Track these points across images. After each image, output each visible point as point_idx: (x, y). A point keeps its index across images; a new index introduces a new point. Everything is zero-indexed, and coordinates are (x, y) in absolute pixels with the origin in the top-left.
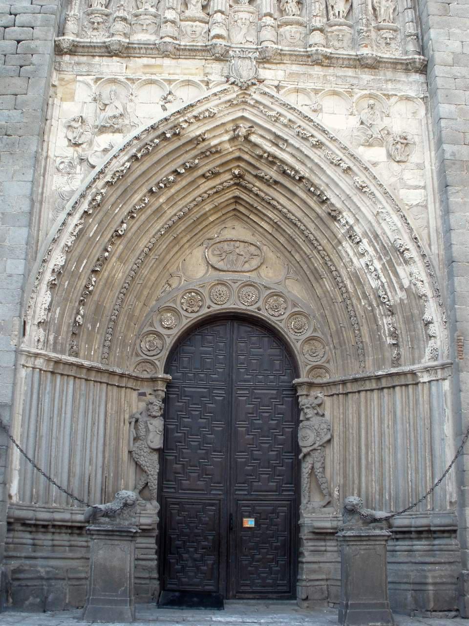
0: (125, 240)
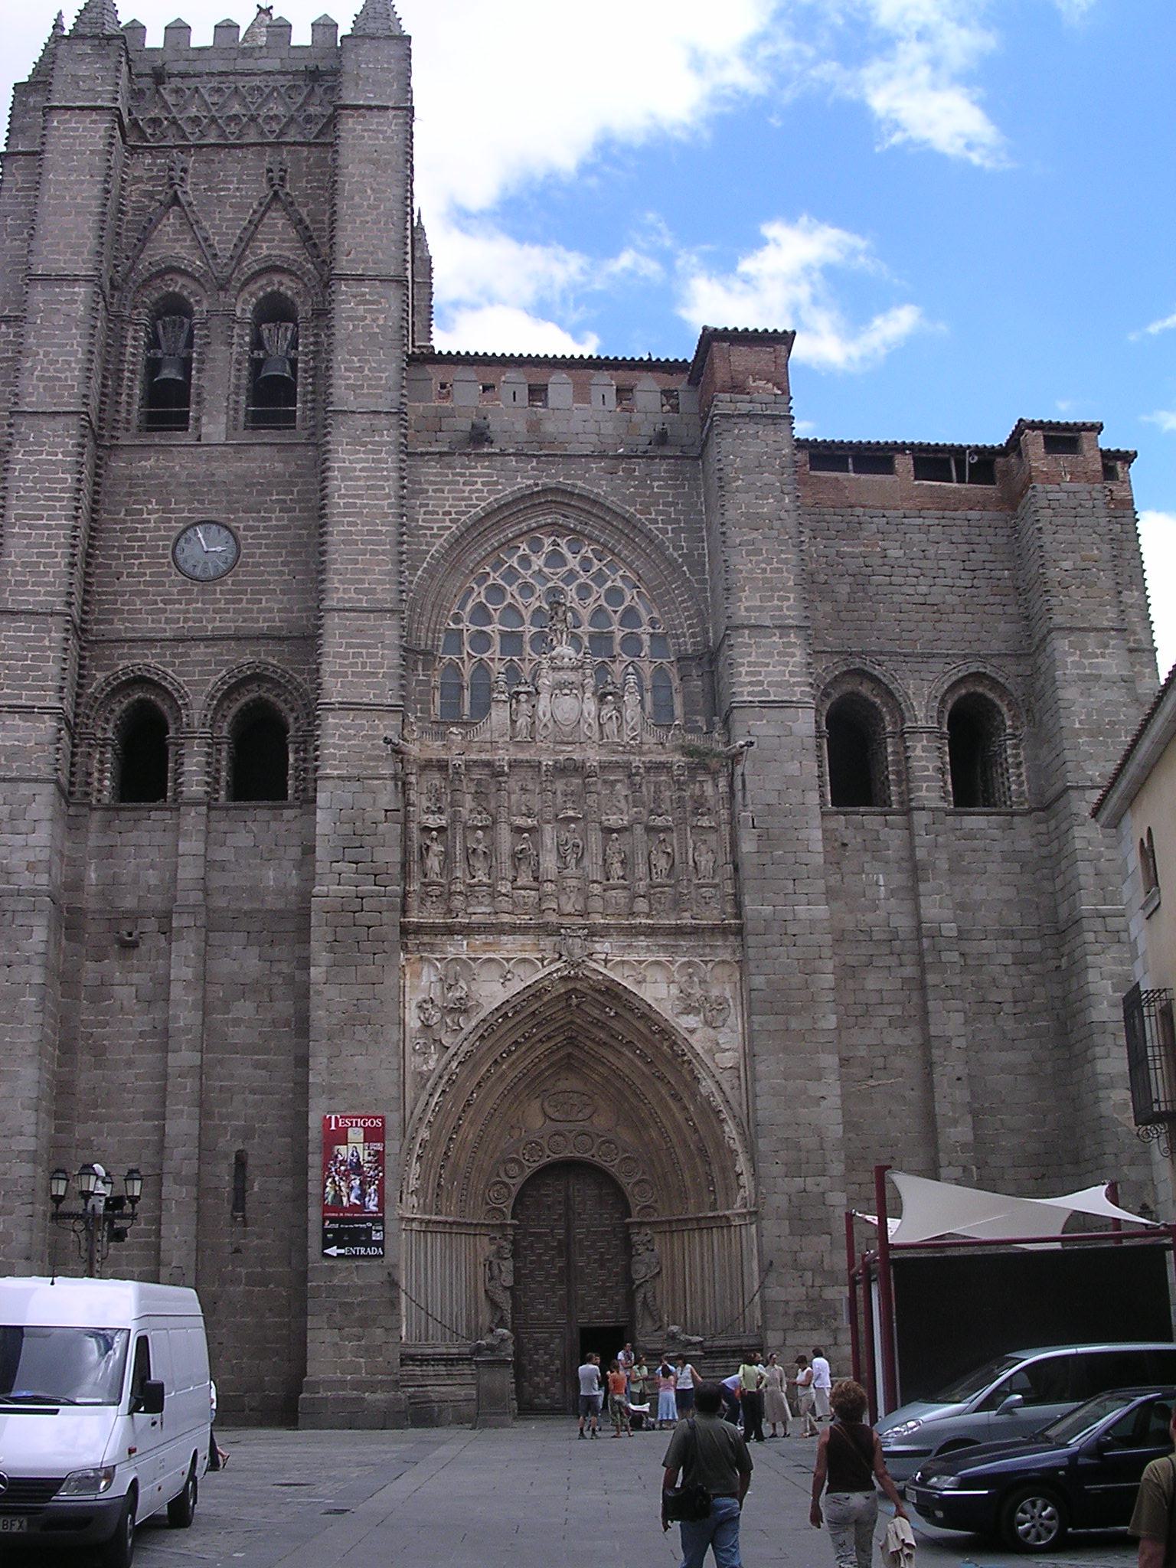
0: (473, 1108)
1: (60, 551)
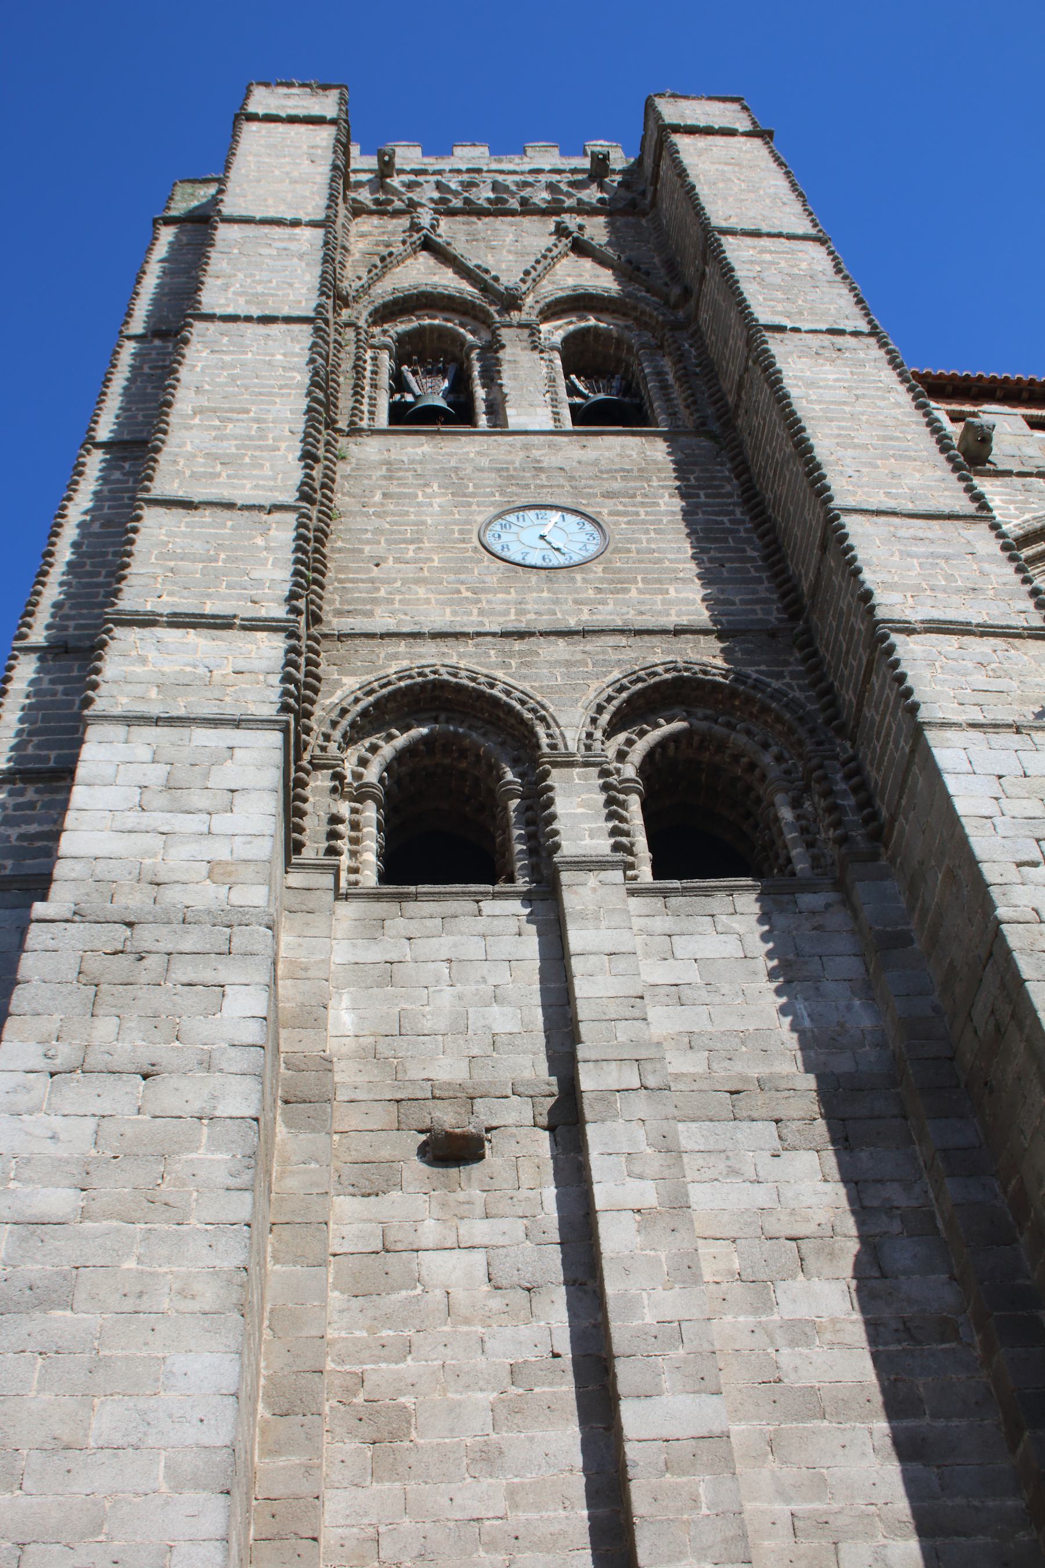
1: (283, 445)
